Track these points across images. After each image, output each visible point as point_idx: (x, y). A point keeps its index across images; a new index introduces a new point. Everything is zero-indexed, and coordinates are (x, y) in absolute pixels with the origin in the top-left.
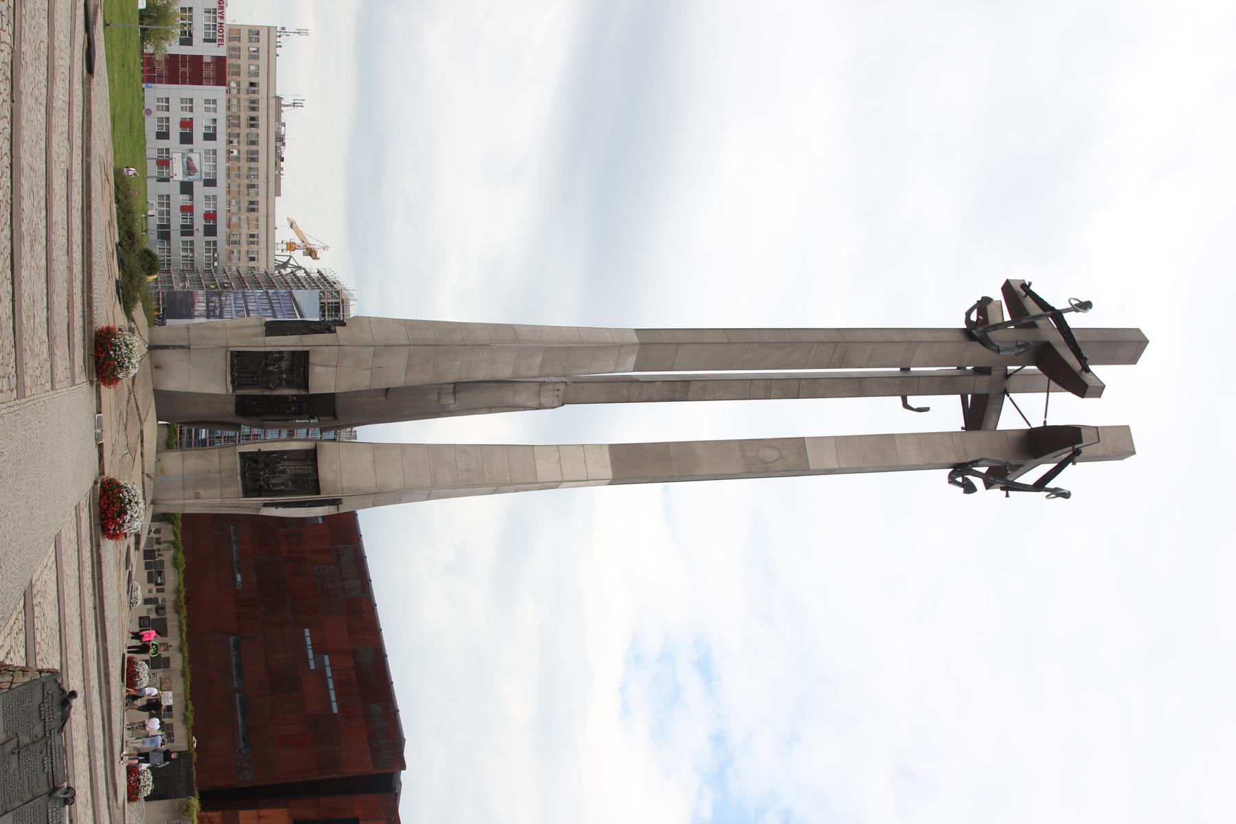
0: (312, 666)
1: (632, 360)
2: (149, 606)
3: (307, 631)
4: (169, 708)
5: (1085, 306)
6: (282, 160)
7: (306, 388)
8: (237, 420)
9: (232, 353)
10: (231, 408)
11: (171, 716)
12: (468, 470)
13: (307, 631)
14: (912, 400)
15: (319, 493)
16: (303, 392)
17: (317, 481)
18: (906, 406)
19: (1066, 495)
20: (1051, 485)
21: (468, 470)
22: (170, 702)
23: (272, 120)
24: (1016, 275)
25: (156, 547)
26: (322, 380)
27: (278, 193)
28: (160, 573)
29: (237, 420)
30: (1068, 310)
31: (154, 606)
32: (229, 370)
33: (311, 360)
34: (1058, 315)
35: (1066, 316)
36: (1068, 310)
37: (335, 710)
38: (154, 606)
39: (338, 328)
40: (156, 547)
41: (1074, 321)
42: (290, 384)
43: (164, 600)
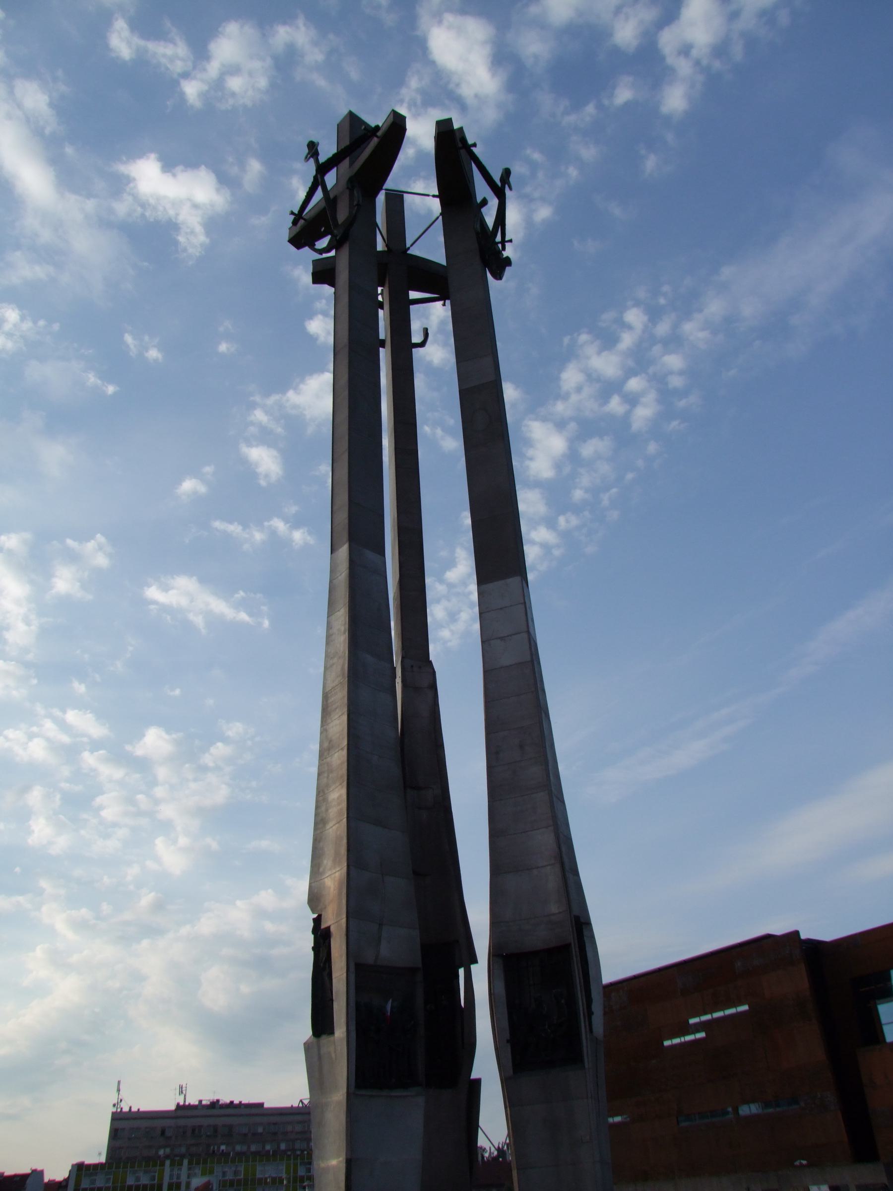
0: (701, 1035)
1: (370, 555)
3: (667, 1043)
5: (313, 149)
6: (232, 1102)
12: (521, 747)
13: (667, 1043)
14: (416, 338)
15: (570, 944)
17: (550, 951)
18: (422, 344)
19: (507, 173)
20: (499, 184)
21: (521, 747)
23: (195, 1113)
24: (286, 235)
27: (261, 1105)
30: (317, 161)
34: (322, 169)
35: (322, 159)
36: (317, 161)
37: (745, 1008)
39: (324, 926)
41: (328, 150)
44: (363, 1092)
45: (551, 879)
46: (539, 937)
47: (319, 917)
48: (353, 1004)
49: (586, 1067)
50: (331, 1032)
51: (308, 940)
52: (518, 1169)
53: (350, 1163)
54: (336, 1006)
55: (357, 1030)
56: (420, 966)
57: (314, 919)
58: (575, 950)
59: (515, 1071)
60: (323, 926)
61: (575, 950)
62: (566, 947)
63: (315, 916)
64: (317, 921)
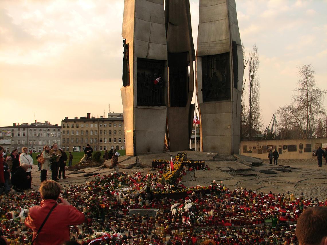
2: (282, 152)
7: (163, 61)
8: (188, 107)
9: (138, 105)
10: (181, 109)
16: (167, 64)
26: (158, 51)
29: (188, 107)
31: (282, 150)
32: (151, 107)
33: (145, 57)
38: (282, 150)
39: (127, 43)
40: (257, 149)
42: (161, 73)
44: (139, 107)
45: (223, 25)
46: (217, 50)
47: (126, 40)
48: (136, 73)
49: (231, 101)
50: (129, 85)
51: (122, 49)
52: (202, 136)
53: (134, 131)
54: (130, 73)
55: (138, 83)
56: (166, 59)
57: (124, 41)
58: (231, 55)
59: (203, 102)
60: (127, 43)
61: (231, 55)
62: (228, 54)
63: (124, 39)
64: (125, 41)
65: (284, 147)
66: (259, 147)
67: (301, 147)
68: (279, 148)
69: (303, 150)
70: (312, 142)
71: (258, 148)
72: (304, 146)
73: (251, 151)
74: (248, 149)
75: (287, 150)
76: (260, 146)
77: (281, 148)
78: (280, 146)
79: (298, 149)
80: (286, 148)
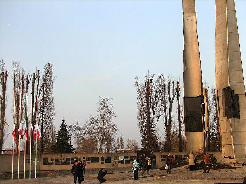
4: (125, 157)
11: (128, 157)
22: (123, 157)
25: (60, 160)
28: (72, 159)
40: (60, 160)
43: (84, 158)
65: (88, 159)
66: (62, 159)
67: (103, 159)
68: (84, 159)
69: (104, 161)
70: (112, 155)
71: (61, 160)
72: (105, 158)
73: (53, 163)
74: (49, 161)
75: (90, 161)
76: (64, 158)
77: (85, 159)
78: (84, 158)
79: (100, 161)
80: (90, 160)
